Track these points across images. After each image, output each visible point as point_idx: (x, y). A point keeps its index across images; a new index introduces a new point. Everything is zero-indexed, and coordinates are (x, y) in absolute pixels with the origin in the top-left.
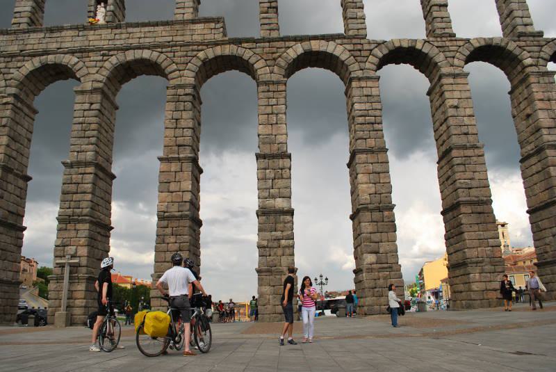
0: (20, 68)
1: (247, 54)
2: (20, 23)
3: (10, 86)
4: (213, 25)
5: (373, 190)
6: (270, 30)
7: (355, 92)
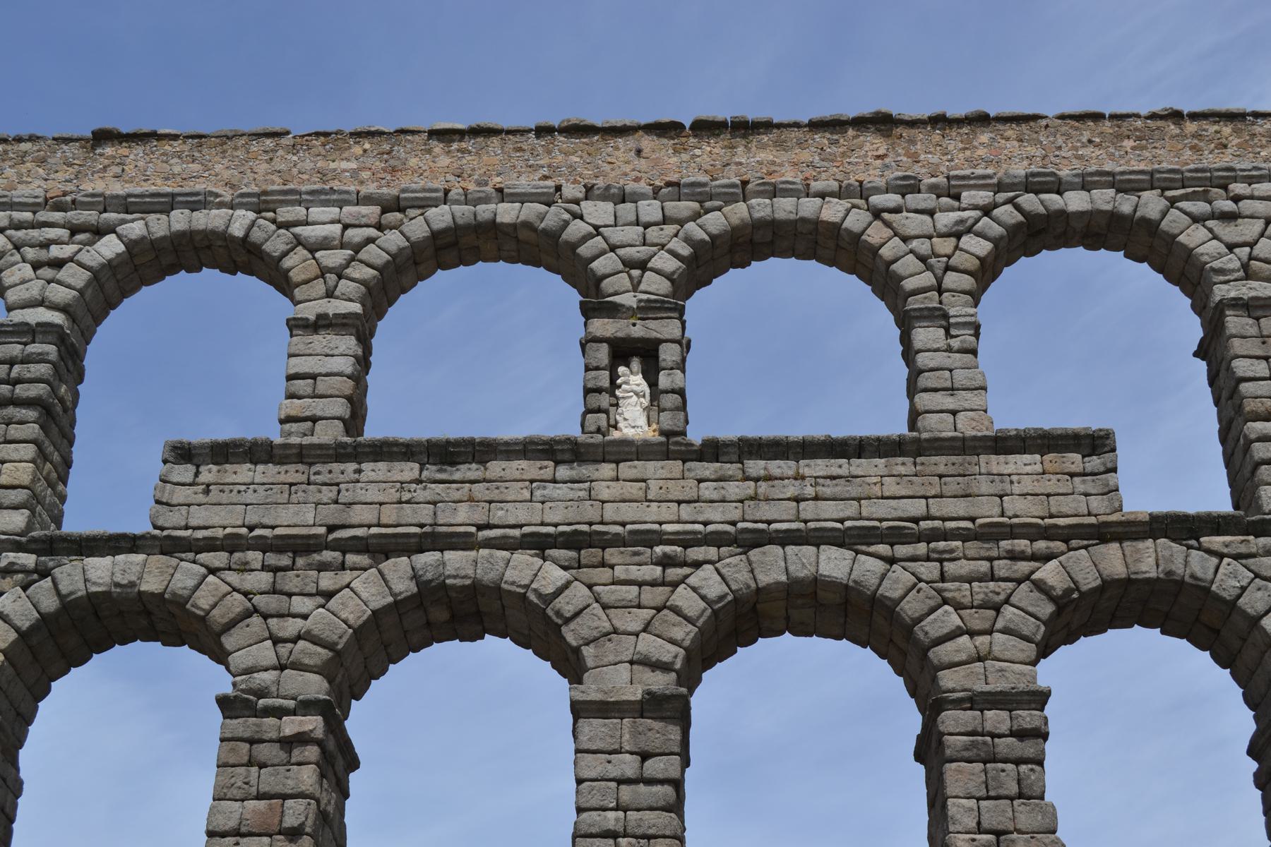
0: (329, 595)
2: (314, 420)
3: (298, 666)
4: (1074, 460)
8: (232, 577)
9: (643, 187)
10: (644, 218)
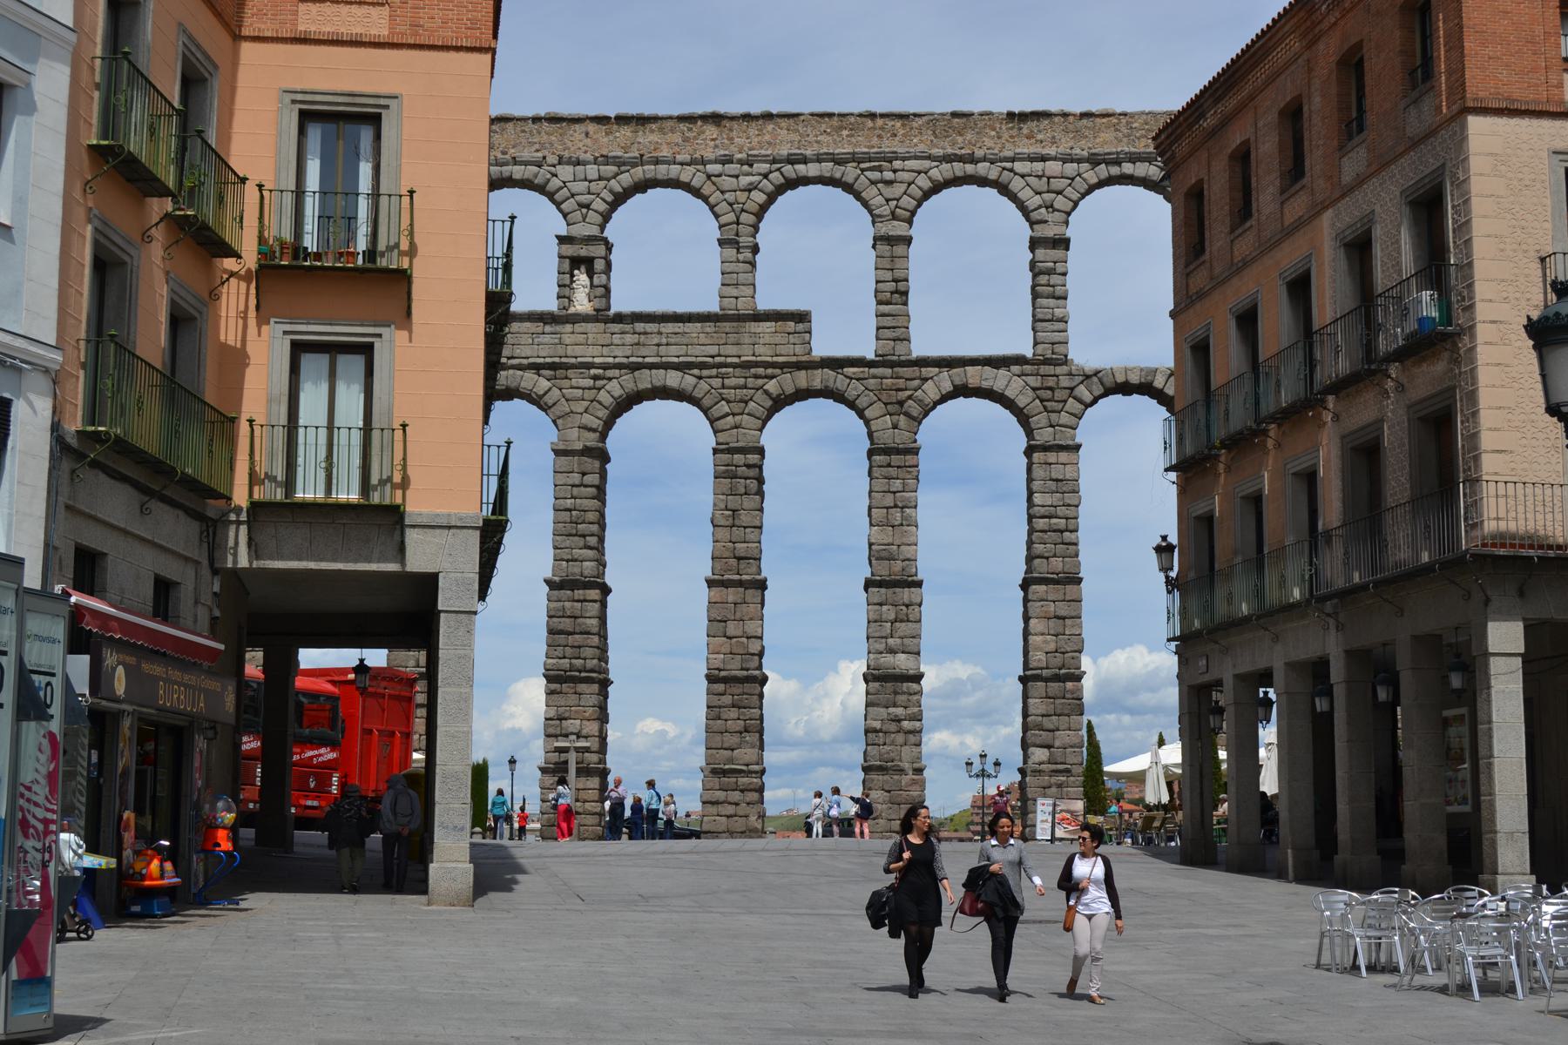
1: (853, 390)
5: (1052, 647)
7: (1038, 472)
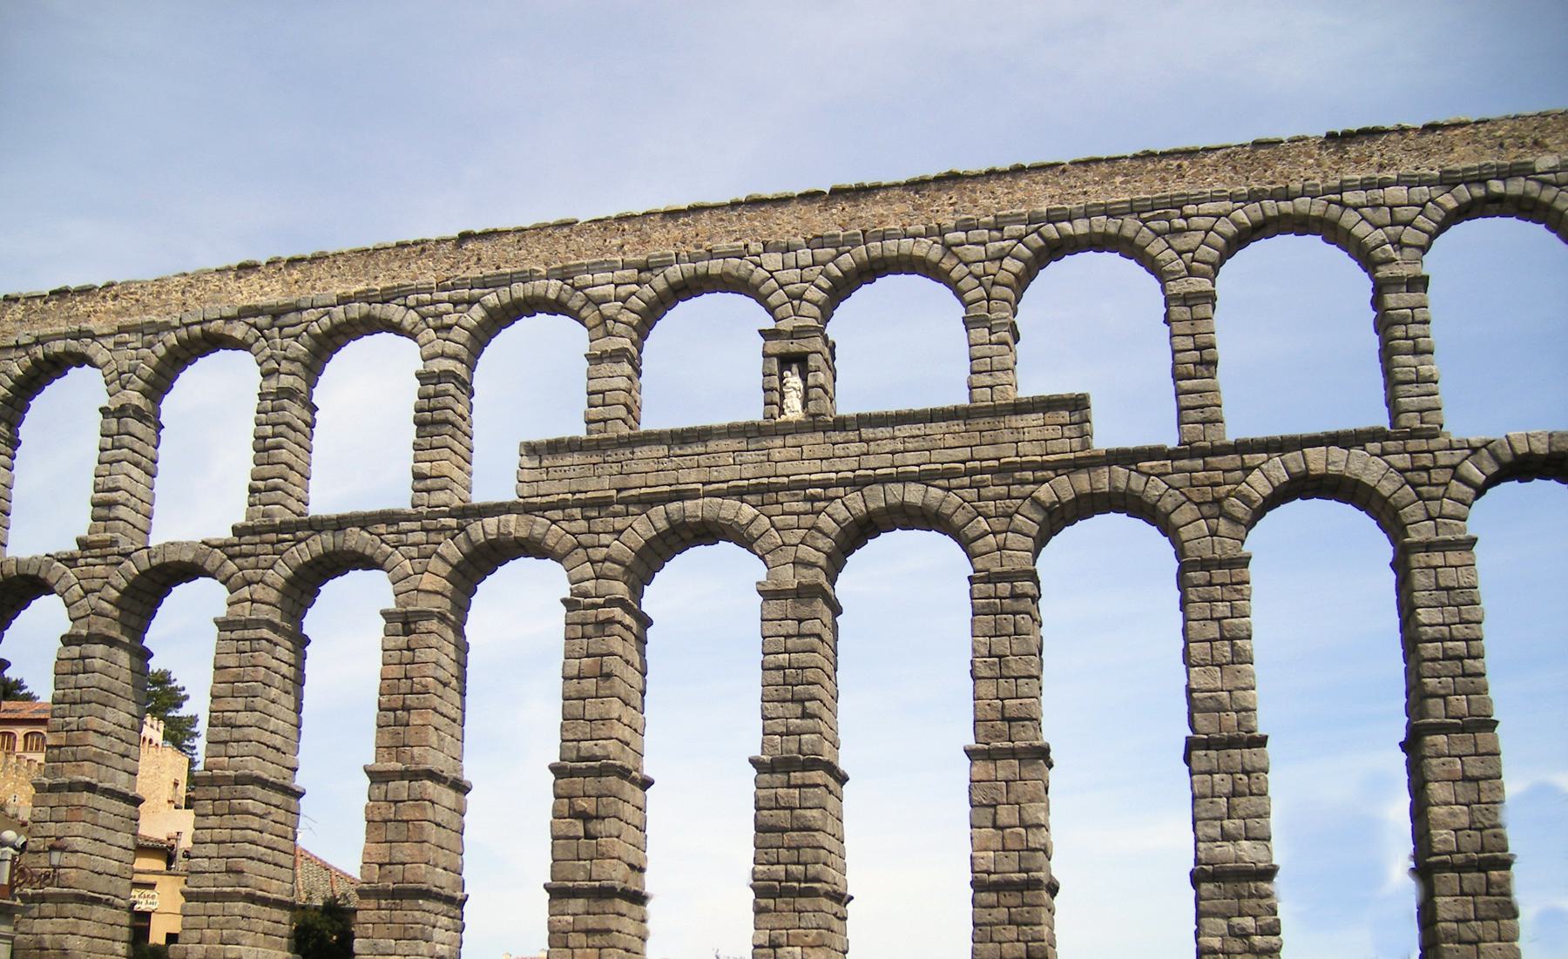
0: (621, 532)
2: (605, 421)
4: (1064, 416)
5: (1464, 820)
6: (1203, 423)
7: (1420, 579)
8: (565, 525)
9: (800, 240)
10: (801, 263)
